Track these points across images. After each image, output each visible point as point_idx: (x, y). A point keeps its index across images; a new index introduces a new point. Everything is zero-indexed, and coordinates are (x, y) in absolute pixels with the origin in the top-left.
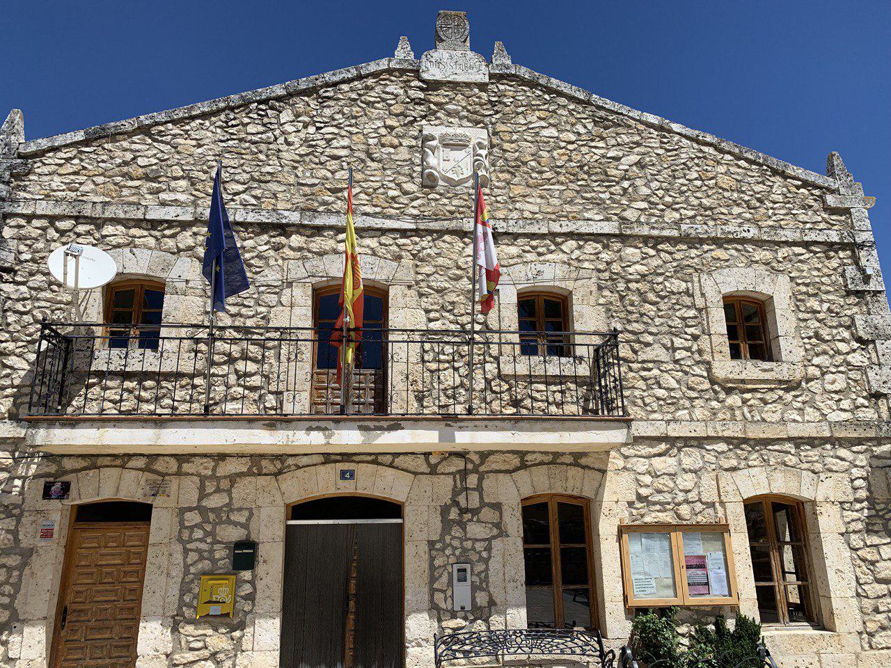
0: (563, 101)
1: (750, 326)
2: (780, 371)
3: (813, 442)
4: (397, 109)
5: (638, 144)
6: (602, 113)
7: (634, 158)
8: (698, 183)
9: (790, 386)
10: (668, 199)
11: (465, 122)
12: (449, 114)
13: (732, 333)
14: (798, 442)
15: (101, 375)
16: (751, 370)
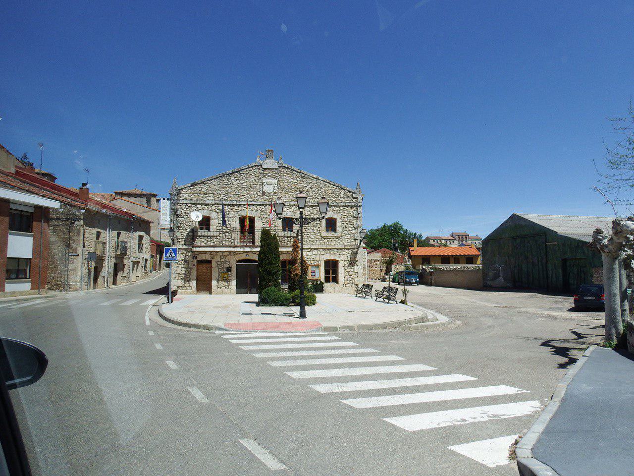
0: (295, 172)
1: (331, 224)
2: (336, 235)
3: (340, 249)
4: (257, 175)
5: (311, 183)
6: (303, 175)
7: (310, 186)
8: (324, 192)
9: (338, 238)
10: (316, 196)
11: (272, 178)
12: (268, 176)
13: (327, 226)
14: (337, 249)
15: (200, 236)
16: (330, 234)
